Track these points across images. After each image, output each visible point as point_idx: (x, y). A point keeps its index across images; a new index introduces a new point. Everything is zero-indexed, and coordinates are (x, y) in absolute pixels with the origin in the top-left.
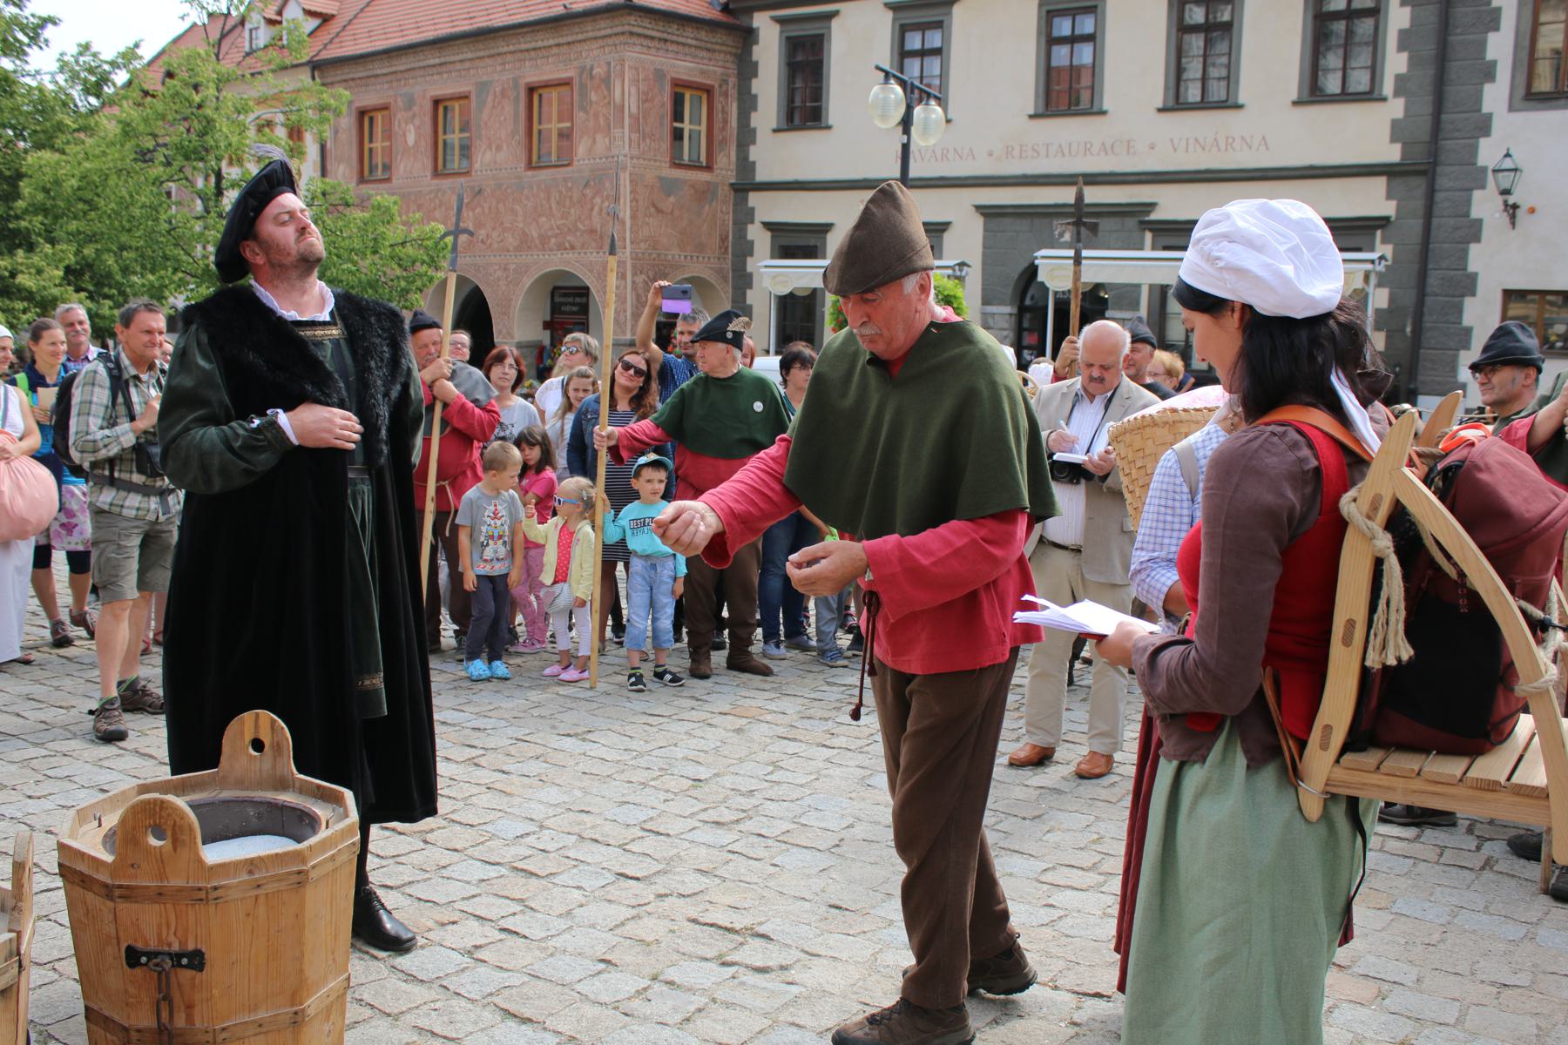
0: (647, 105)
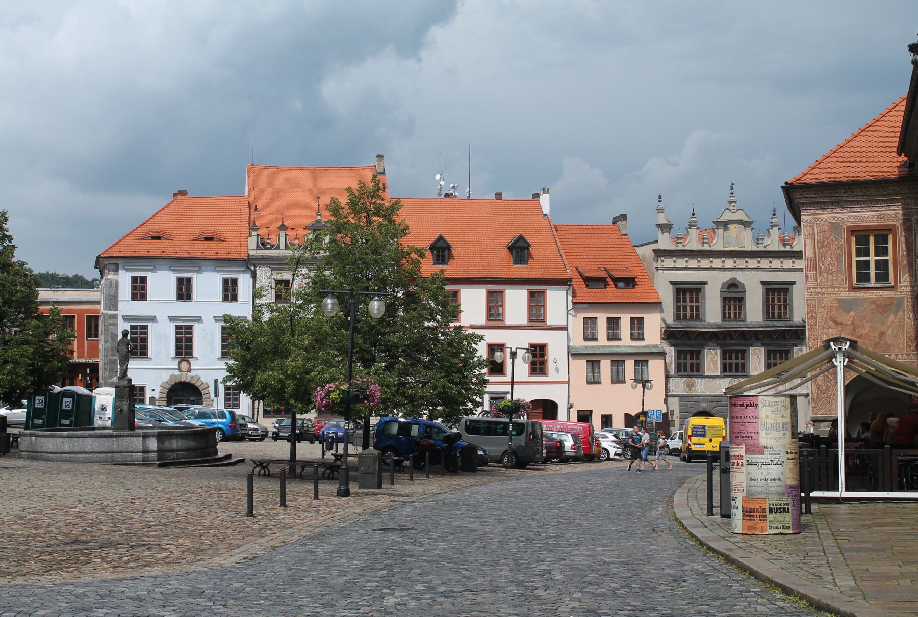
0: (823, 249)
